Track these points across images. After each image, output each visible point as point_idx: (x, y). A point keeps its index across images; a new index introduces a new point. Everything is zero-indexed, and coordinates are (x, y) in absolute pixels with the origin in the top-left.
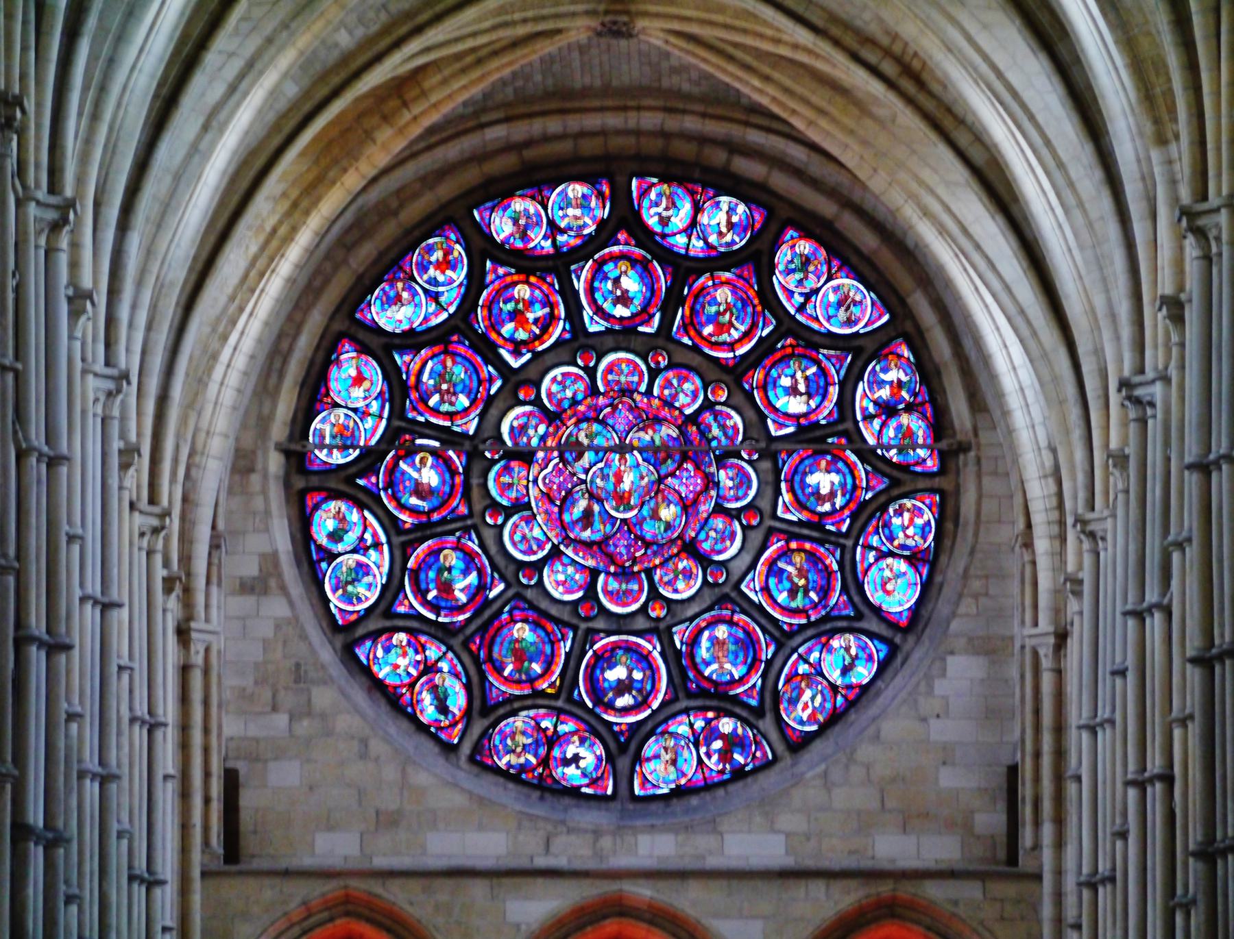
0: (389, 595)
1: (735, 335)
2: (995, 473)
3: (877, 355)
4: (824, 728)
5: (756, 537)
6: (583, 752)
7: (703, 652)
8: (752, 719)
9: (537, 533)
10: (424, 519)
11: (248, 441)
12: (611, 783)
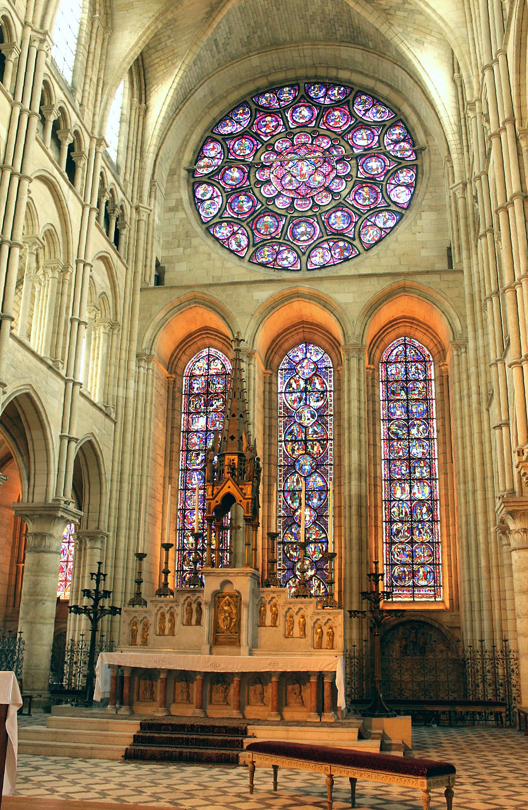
0: (221, 212)
1: (341, 124)
2: (435, 154)
3: (391, 126)
4: (377, 243)
5: (351, 184)
6: (289, 255)
7: (332, 221)
8: (351, 241)
9: (273, 188)
10: (234, 187)
11: (174, 167)
12: (299, 265)
